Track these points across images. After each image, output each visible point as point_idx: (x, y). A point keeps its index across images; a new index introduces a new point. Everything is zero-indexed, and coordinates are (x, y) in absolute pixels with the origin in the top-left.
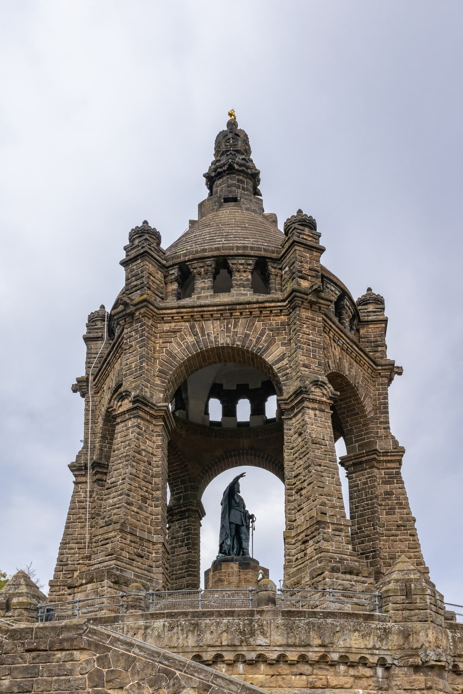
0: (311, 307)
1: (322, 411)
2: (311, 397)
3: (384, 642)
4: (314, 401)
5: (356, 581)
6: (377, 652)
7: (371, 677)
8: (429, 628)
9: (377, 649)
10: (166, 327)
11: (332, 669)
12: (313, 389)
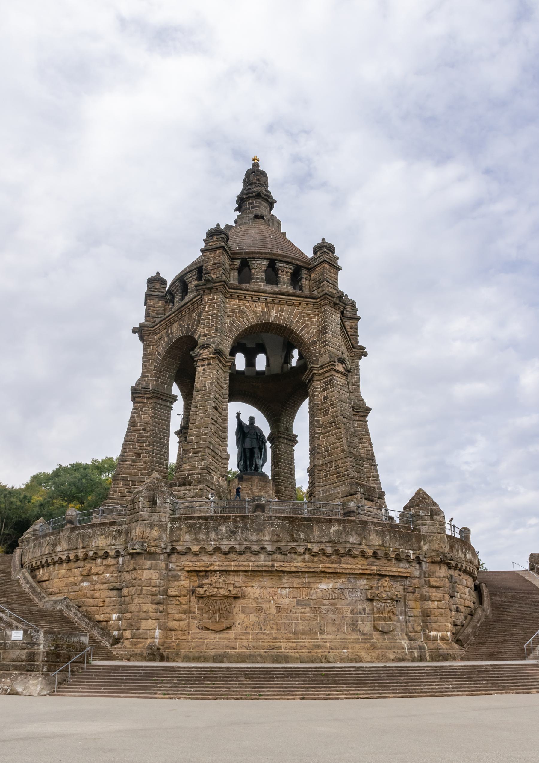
0: (211, 291)
1: (209, 364)
2: (201, 357)
4: (204, 359)
5: (189, 490)
6: (114, 547)
7: (114, 565)
8: (137, 526)
9: (113, 545)
10: (158, 336)
11: (94, 562)
12: (201, 352)
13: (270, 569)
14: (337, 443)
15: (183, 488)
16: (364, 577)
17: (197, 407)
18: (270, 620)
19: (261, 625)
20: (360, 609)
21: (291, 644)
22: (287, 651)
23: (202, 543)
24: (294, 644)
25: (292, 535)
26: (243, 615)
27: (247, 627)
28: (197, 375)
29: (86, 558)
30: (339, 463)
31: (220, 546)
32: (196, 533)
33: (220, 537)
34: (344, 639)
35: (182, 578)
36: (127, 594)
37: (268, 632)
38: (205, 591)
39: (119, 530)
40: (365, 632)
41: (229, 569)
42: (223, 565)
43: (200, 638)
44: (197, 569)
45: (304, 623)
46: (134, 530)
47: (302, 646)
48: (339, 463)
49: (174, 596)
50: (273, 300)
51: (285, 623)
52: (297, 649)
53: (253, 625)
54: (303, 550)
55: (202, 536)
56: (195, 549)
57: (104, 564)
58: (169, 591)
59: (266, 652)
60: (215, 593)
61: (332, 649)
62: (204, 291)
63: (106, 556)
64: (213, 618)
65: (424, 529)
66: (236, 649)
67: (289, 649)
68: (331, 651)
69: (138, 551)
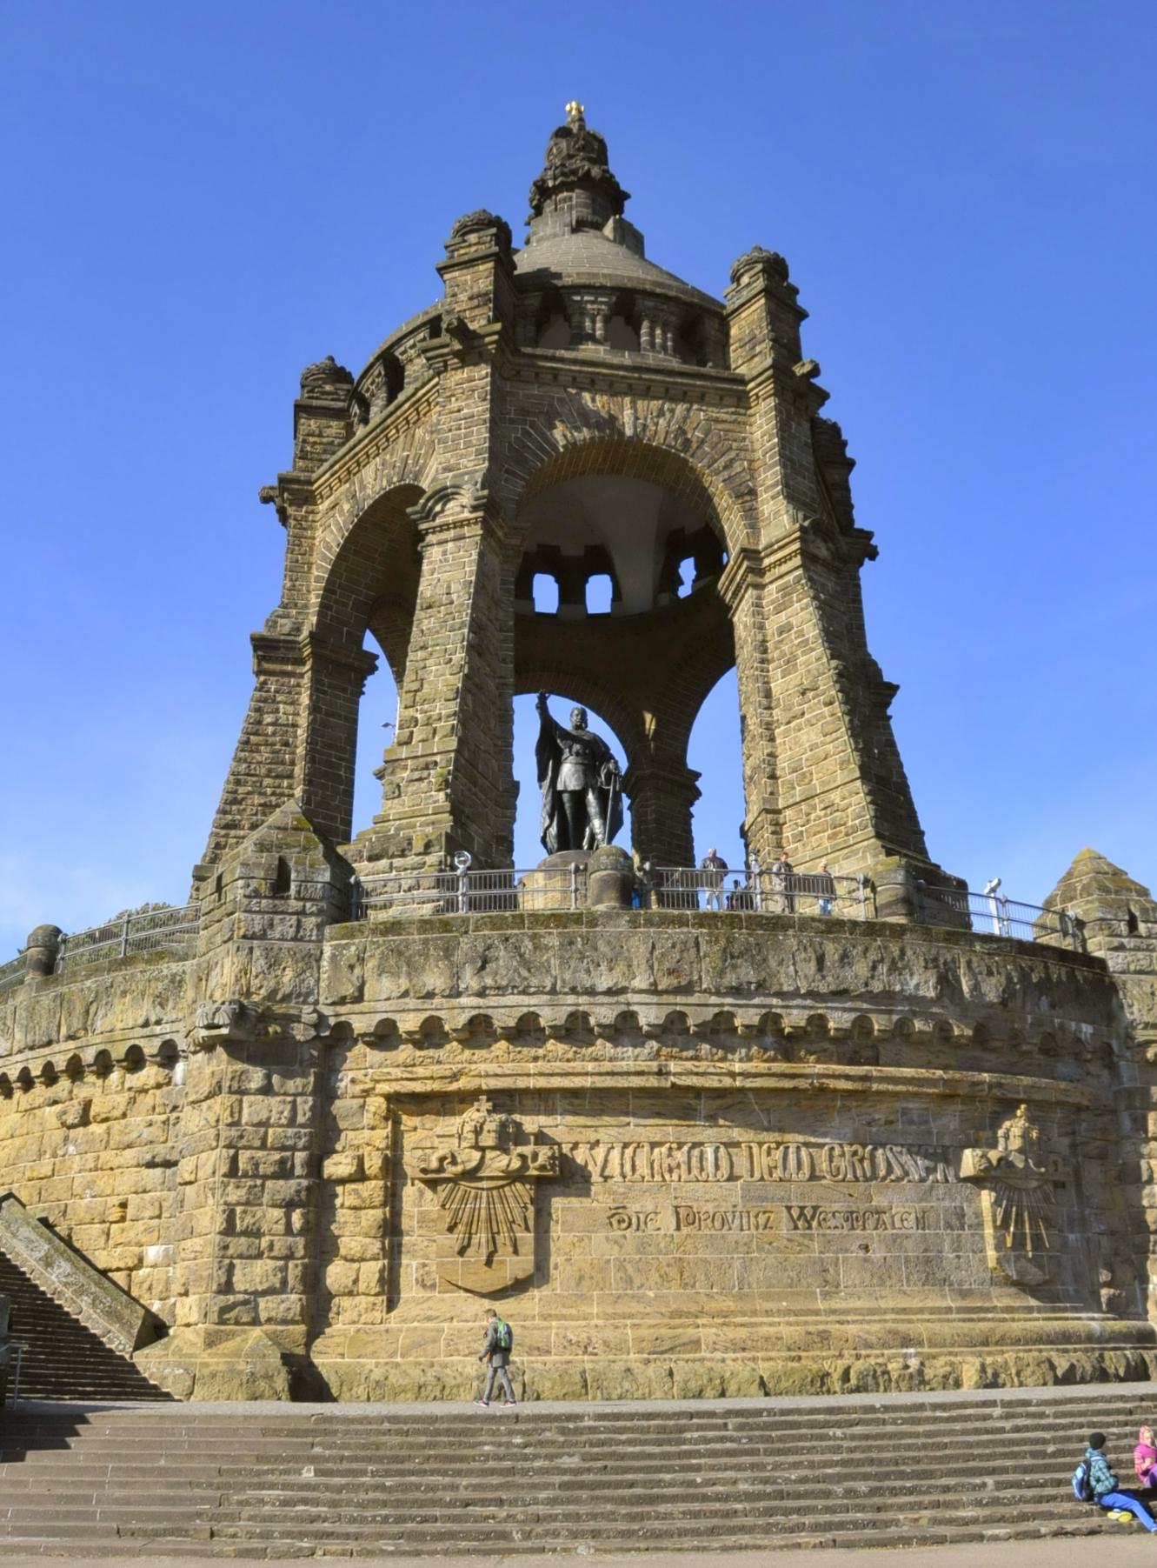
2: (438, 521)
3: (171, 1004)
4: (445, 527)
6: (158, 1029)
9: (158, 1023)
10: (327, 503)
13: (652, 1082)
14: (824, 744)
15: (384, 863)
16: (953, 1107)
17: (423, 648)
18: (660, 1252)
19: (630, 1270)
20: (946, 1210)
21: (731, 1333)
22: (718, 1355)
23: (437, 1001)
24: (742, 1333)
25: (721, 974)
26: (570, 1237)
27: (581, 1278)
28: (425, 567)
29: (75, 1070)
30: (835, 797)
31: (489, 1012)
32: (414, 970)
33: (489, 981)
34: (904, 1311)
35: (368, 1119)
36: (192, 1178)
37: (651, 1294)
38: (442, 1159)
39: (174, 976)
40: (966, 1287)
41: (522, 1083)
42: (499, 1071)
43: (429, 1319)
44: (418, 1087)
45: (771, 1259)
46: (218, 970)
47: (767, 1339)
48: (835, 797)
49: (343, 1181)
50: (630, 386)
51: (705, 1261)
52: (754, 1348)
53: (602, 1270)
54: (756, 1020)
55: (435, 979)
56: (409, 1023)
57: (127, 1085)
58: (326, 1163)
59: (648, 1361)
60: (473, 1164)
61: (869, 1346)
62: (445, 362)
63: (135, 1060)
64: (470, 1252)
65: (1115, 962)
66: (548, 1352)
67: (726, 1350)
68: (863, 1352)
69: (225, 1031)
